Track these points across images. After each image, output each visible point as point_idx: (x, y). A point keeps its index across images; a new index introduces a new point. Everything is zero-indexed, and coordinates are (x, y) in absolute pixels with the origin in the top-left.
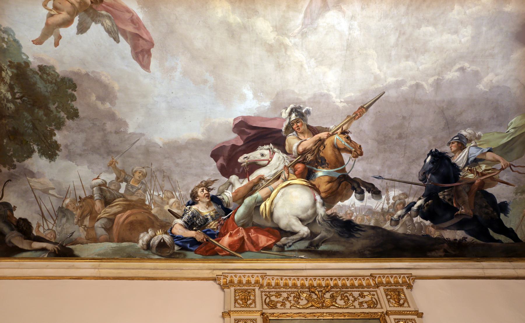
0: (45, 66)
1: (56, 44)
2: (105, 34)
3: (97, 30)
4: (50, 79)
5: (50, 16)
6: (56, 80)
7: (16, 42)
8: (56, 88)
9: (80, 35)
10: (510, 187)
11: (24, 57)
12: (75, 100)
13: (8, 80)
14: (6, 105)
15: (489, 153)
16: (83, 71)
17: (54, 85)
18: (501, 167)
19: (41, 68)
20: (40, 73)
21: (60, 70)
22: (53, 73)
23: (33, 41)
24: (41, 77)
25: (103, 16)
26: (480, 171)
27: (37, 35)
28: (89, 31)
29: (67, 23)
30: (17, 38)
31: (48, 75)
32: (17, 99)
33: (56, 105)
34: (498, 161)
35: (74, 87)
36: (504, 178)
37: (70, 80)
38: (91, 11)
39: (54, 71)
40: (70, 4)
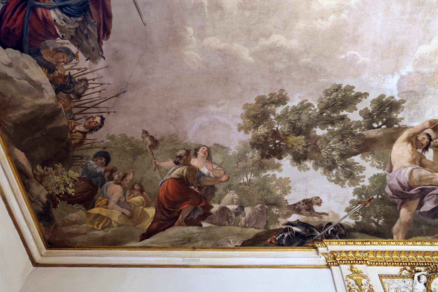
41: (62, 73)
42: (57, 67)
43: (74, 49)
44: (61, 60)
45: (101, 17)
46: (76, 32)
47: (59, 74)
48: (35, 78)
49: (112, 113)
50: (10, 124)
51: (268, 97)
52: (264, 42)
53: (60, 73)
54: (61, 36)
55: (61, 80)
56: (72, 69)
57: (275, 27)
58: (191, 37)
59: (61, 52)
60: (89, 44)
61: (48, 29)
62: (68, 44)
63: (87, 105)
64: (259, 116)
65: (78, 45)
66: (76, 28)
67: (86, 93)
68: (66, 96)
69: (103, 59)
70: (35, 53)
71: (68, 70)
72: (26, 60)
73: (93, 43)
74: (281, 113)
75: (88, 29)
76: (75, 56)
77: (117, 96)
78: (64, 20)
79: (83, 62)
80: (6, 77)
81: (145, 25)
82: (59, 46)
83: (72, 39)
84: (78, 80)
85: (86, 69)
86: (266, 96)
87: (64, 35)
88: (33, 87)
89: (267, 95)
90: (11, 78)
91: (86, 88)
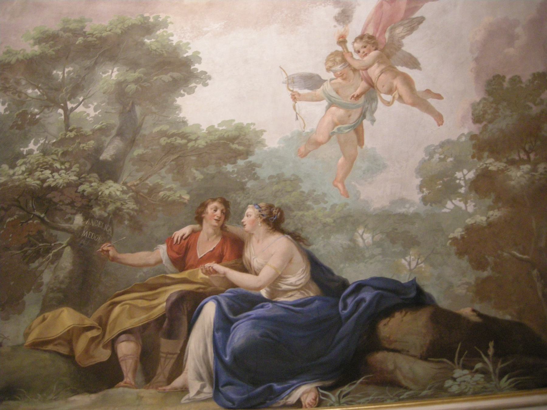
0: (473, 114)
1: (439, 97)
2: (415, 35)
3: (412, 44)
4: (492, 110)
5: (400, 98)
6: (492, 103)
7: (442, 145)
8: (505, 104)
9: (421, 66)
11: (463, 139)
12: (519, 77)
13: (501, 165)
14: (541, 174)
16: (472, 65)
17: (500, 106)
19: (477, 120)
20: (485, 123)
21: (475, 95)
22: (481, 106)
23: (439, 125)
24: (490, 122)
25: (391, 37)
27: (429, 119)
28: (415, 54)
29: (408, 82)
30: (437, 144)
31: (485, 112)
32: (529, 157)
33: (530, 104)
35: (498, 79)
37: (489, 83)
38: (387, 50)
39: (479, 104)
40: (383, 75)
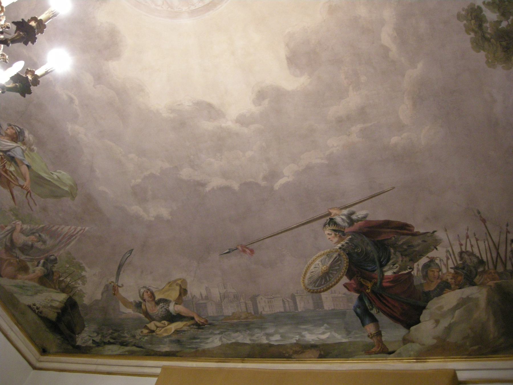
10: (12, 202)
15: (26, 167)
18: (22, 184)
26: (7, 167)
34: (25, 179)
36: (15, 193)
41: (451, 275)
42: (444, 279)
43: (424, 260)
44: (436, 274)
45: (389, 230)
46: (406, 256)
47: (451, 279)
48: (454, 303)
49: (509, 228)
50: (501, 340)
51: (472, 35)
52: (394, 50)
53: (451, 277)
54: (410, 270)
55: (459, 278)
56: (446, 265)
57: (373, 43)
58: (402, 138)
59: (427, 273)
60: (418, 245)
61: (404, 280)
62: (418, 265)
63: (494, 255)
64: (504, 43)
65: (420, 255)
66: (402, 255)
67: (478, 255)
68: (480, 276)
69: (435, 233)
70: (428, 297)
71: (448, 269)
72: (433, 306)
73: (417, 241)
74: (496, 13)
75: (403, 244)
76: (432, 260)
77: (484, 221)
78: (394, 265)
79: (439, 253)
80: (449, 329)
81: (394, 188)
82: (420, 274)
83: (414, 259)
84: (460, 260)
85: (448, 251)
86: (471, 38)
87: (409, 267)
88: (464, 307)
89: (469, 36)
90: (450, 324)
91: (472, 254)
